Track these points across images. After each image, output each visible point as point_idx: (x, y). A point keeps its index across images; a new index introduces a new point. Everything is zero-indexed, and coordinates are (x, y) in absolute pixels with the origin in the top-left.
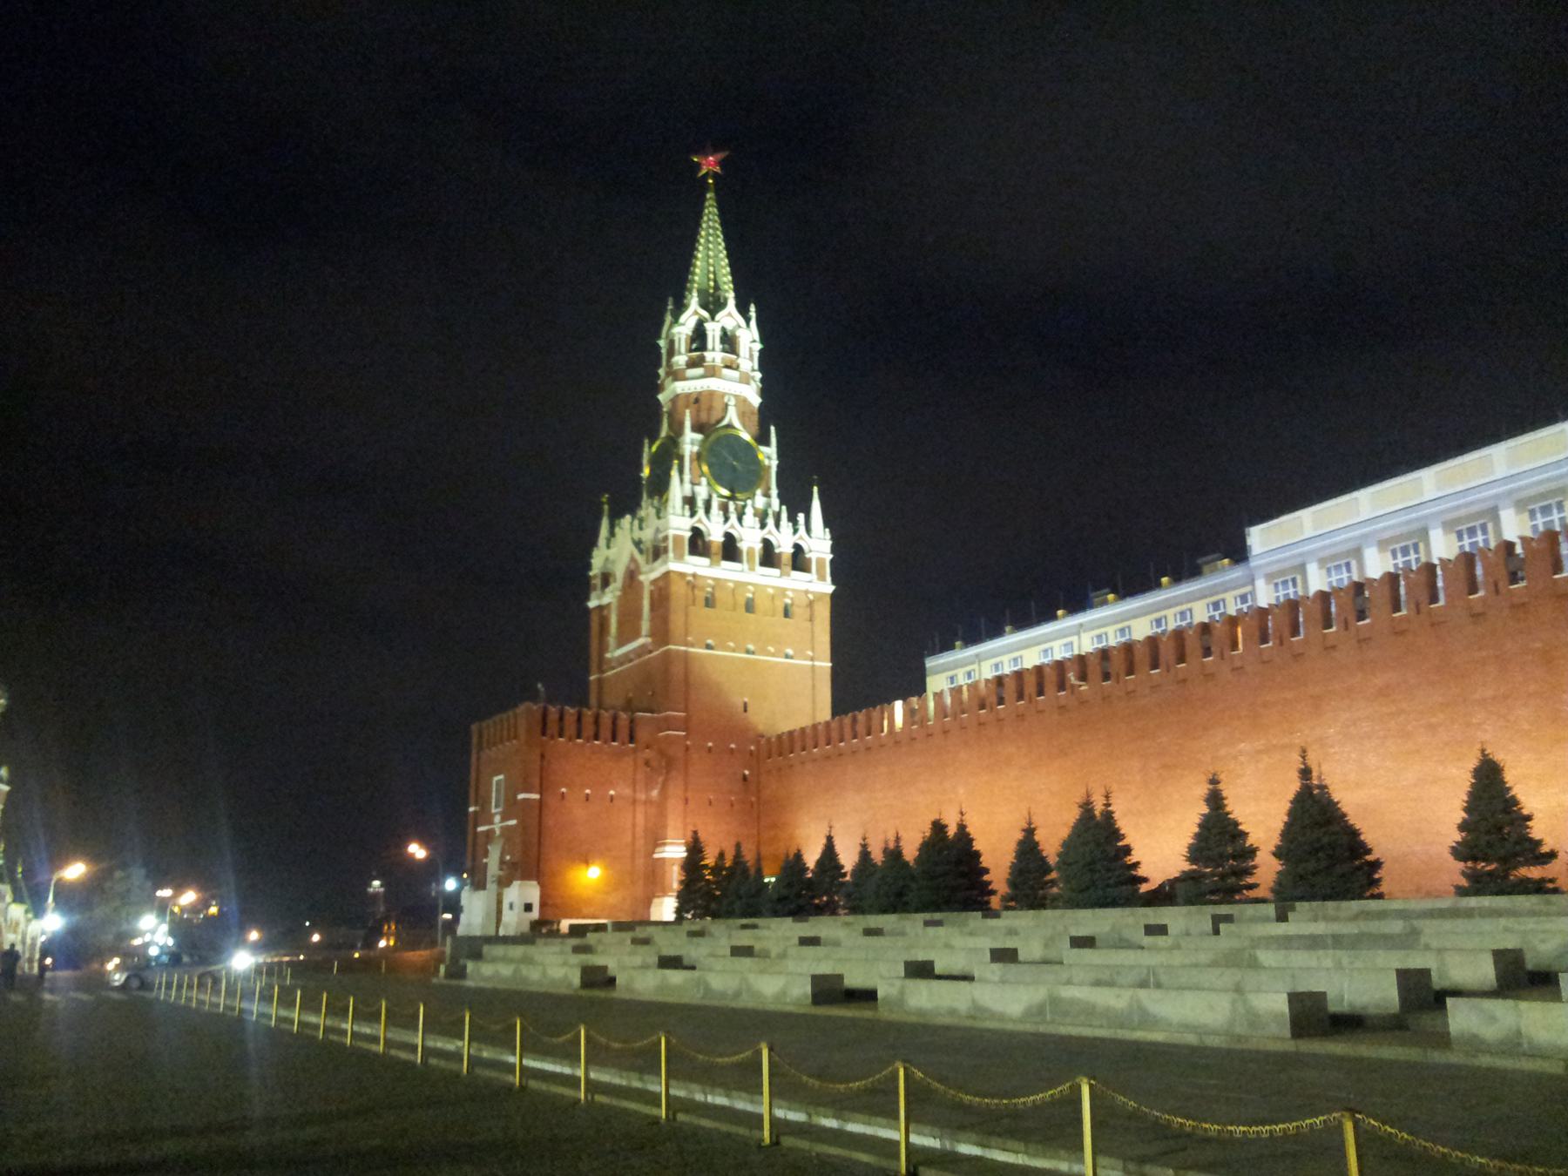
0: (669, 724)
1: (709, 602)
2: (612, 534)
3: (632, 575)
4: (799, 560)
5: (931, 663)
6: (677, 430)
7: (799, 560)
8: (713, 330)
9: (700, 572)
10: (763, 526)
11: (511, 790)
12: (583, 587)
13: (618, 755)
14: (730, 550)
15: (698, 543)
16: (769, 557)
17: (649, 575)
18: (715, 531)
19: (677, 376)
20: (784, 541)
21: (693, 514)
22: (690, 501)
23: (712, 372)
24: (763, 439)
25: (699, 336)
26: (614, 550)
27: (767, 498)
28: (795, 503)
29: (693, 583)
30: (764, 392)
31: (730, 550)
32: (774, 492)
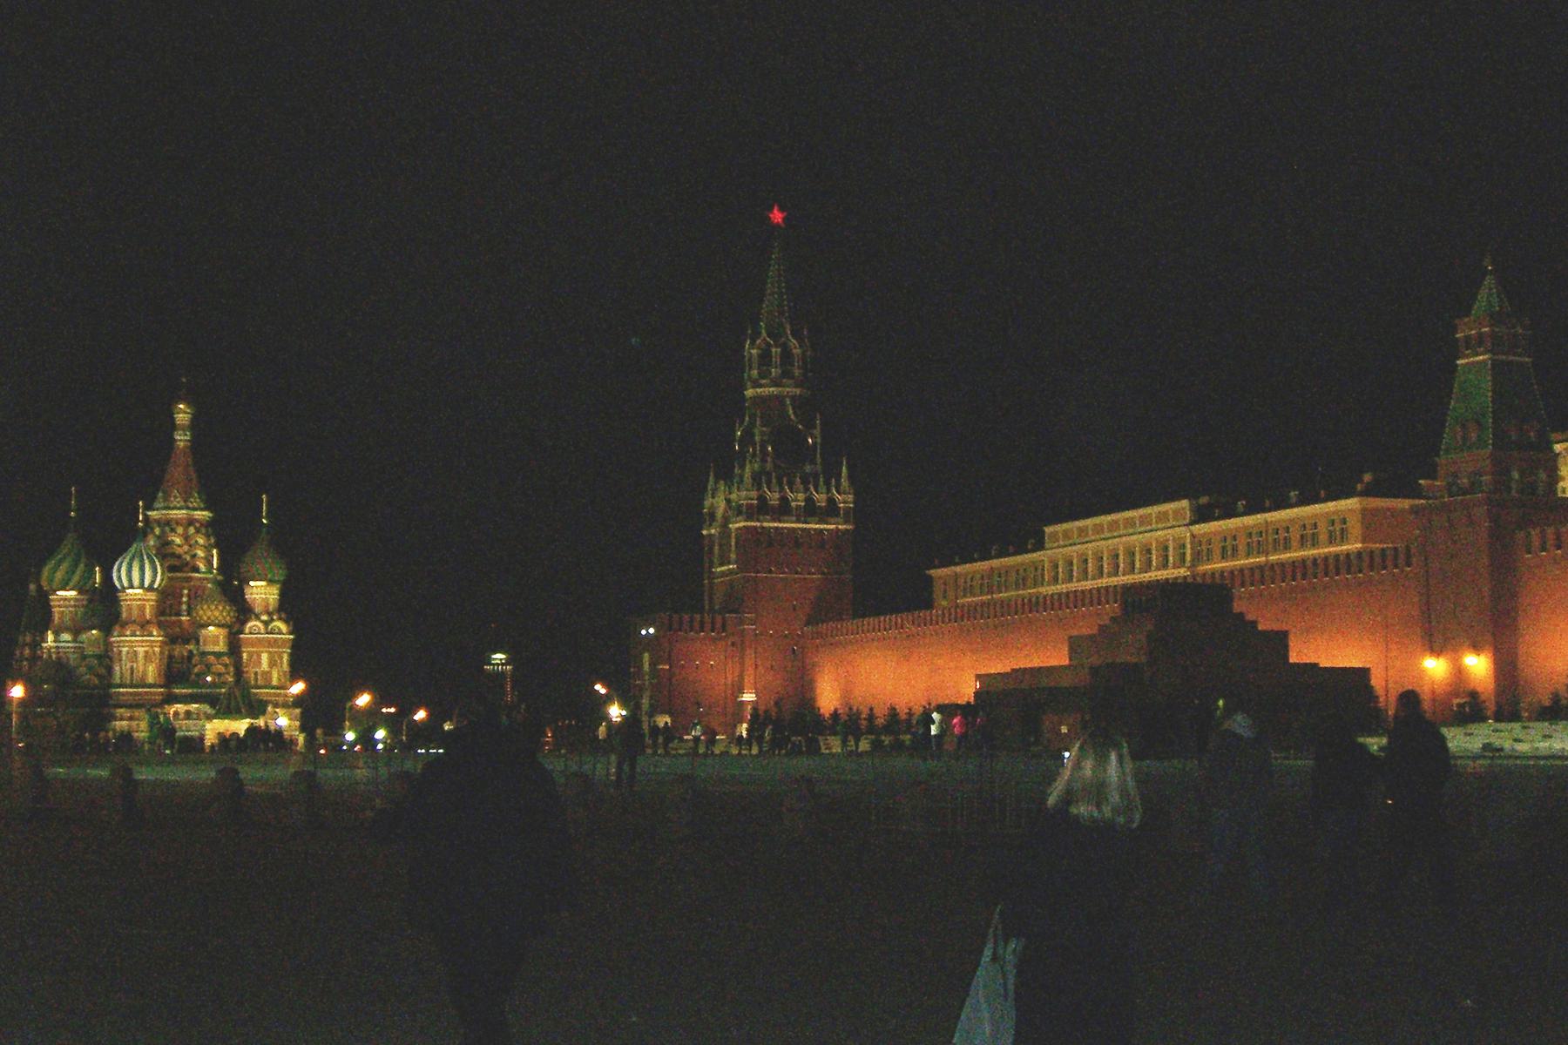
0: (742, 622)
2: (715, 491)
3: (726, 521)
6: (752, 424)
7: (831, 510)
9: (766, 524)
10: (807, 490)
11: (653, 664)
13: (714, 640)
14: (784, 510)
15: (762, 508)
16: (810, 511)
17: (737, 525)
18: (773, 498)
19: (756, 385)
20: (820, 498)
21: (759, 488)
22: (757, 479)
23: (776, 384)
24: (810, 425)
25: (765, 357)
26: (717, 502)
28: (831, 473)
32: (819, 460)
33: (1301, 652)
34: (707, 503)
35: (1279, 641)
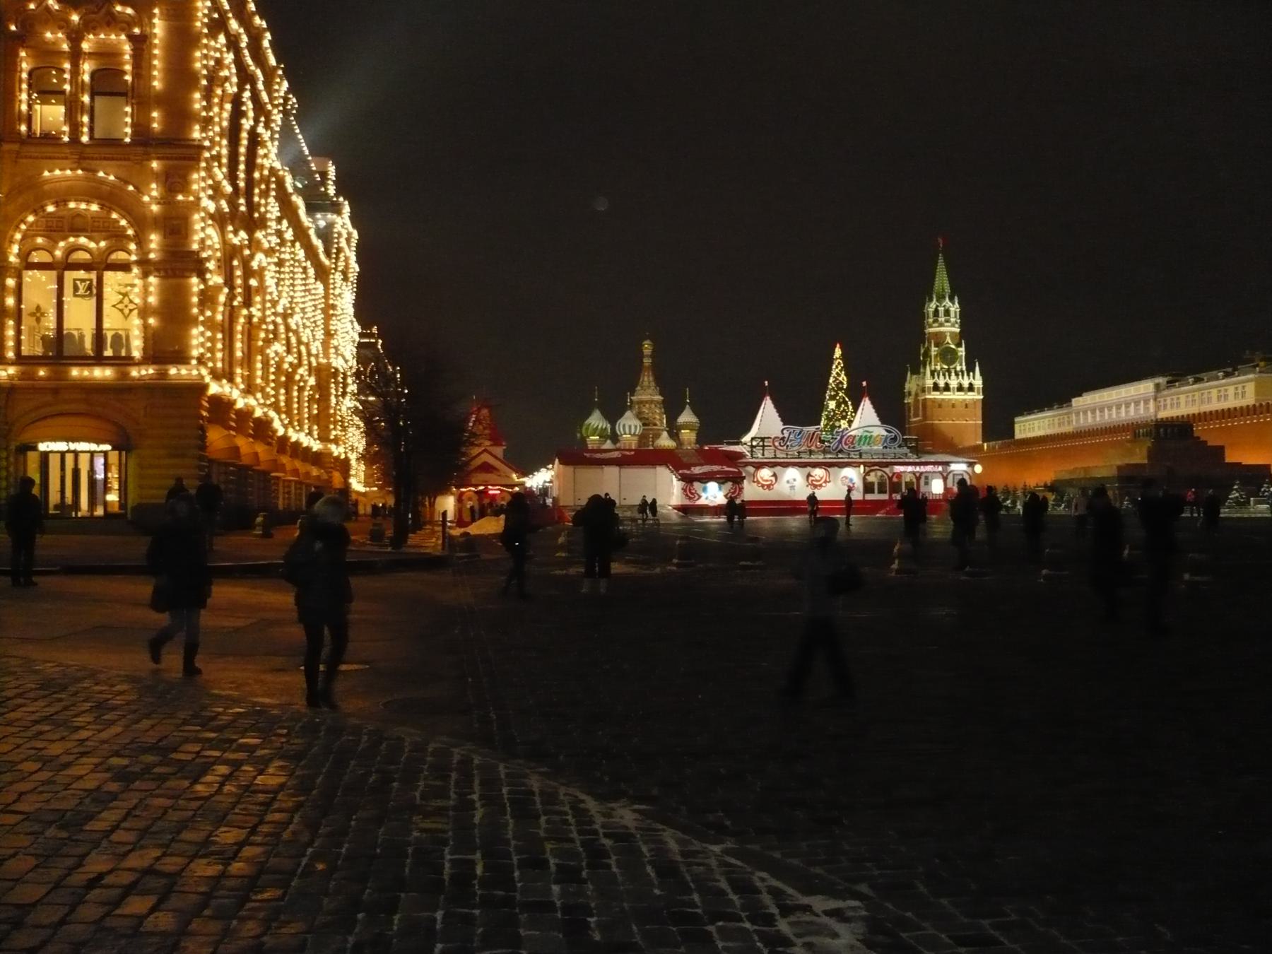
1: (940, 406)
3: (917, 395)
4: (971, 388)
5: (1017, 419)
7: (971, 388)
8: (941, 309)
12: (903, 395)
14: (947, 388)
15: (936, 387)
16: (960, 388)
18: (942, 383)
19: (931, 326)
20: (966, 384)
22: (932, 373)
23: (941, 325)
24: (959, 345)
25: (936, 313)
27: (961, 366)
28: (970, 369)
29: (933, 401)
30: (961, 327)
31: (947, 388)
33: (1231, 457)
34: (907, 386)
35: (1220, 450)
